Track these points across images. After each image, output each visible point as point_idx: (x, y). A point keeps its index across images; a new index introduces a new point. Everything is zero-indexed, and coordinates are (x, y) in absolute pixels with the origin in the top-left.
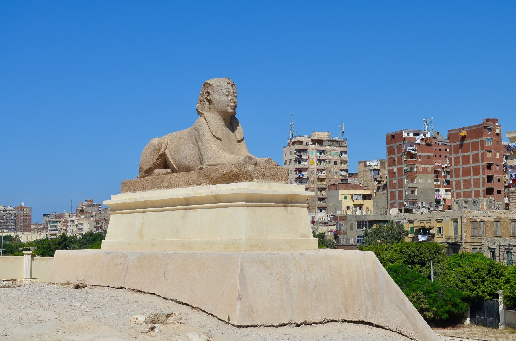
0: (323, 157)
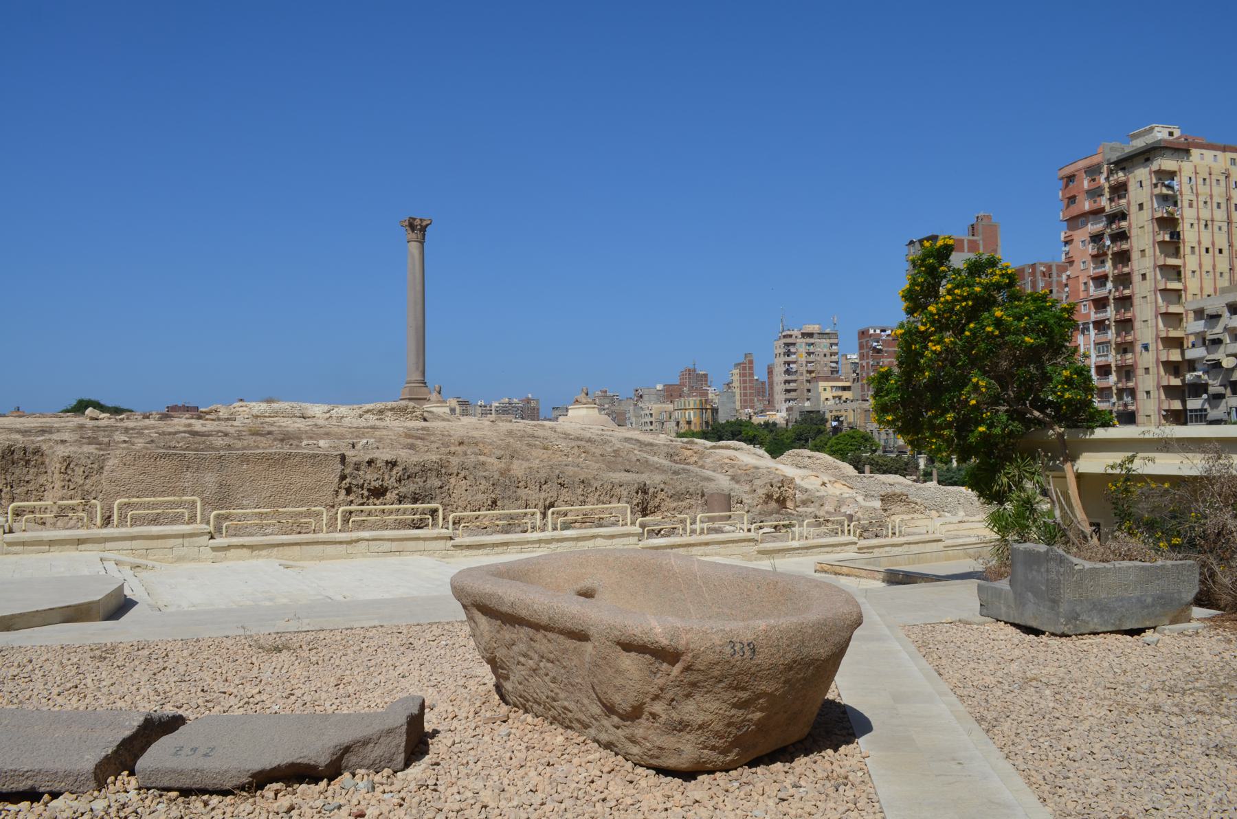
0: (812, 349)
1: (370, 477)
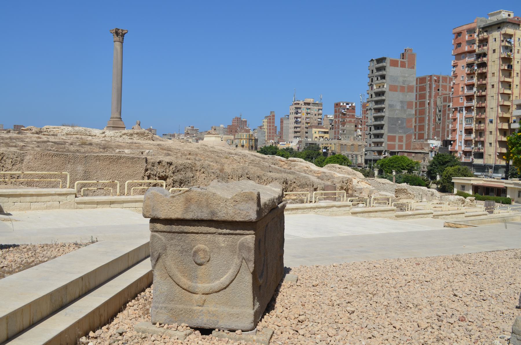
1: (159, 170)
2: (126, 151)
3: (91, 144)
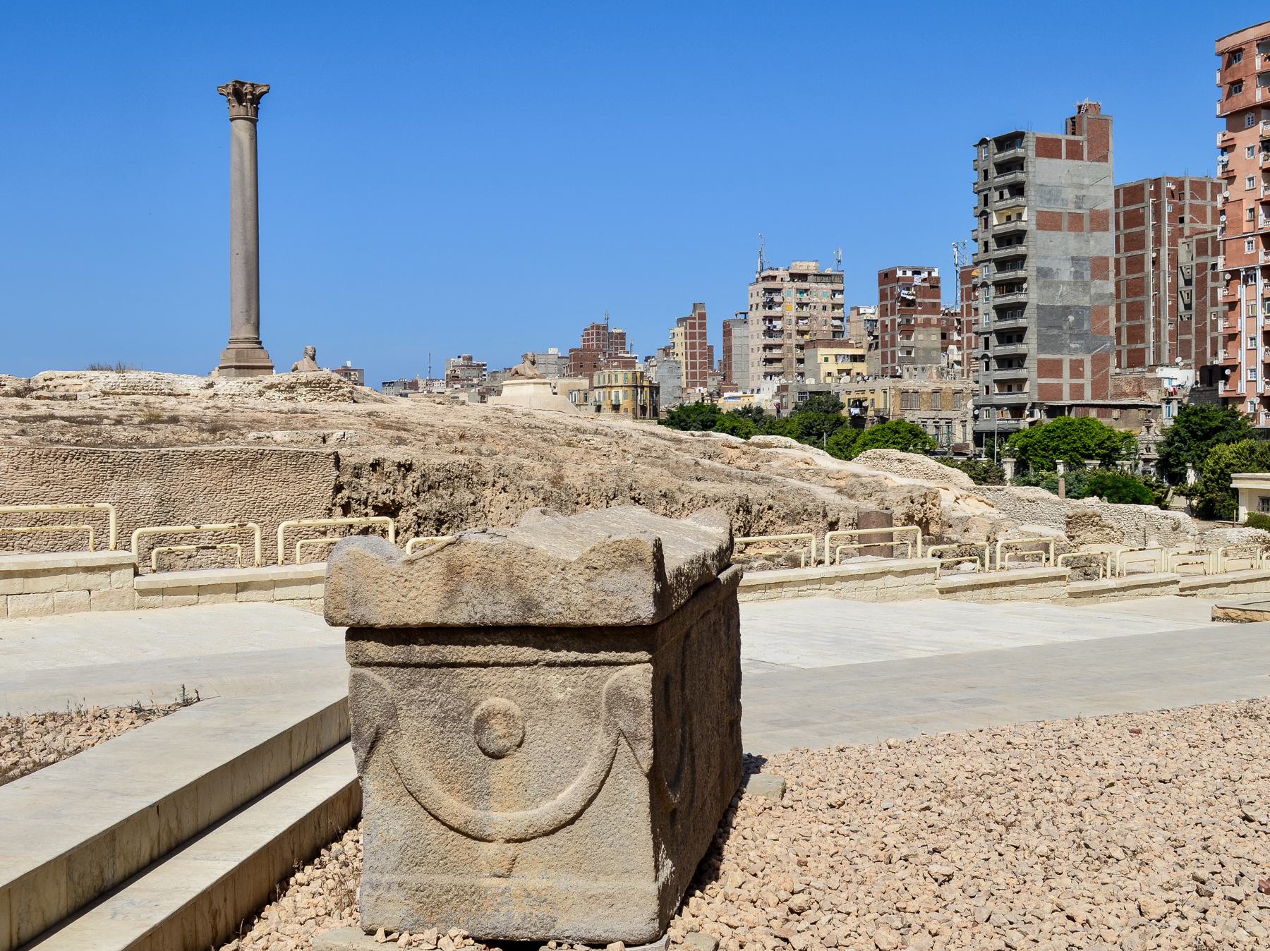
0: (805, 298)
2: (279, 436)
3: (174, 420)
